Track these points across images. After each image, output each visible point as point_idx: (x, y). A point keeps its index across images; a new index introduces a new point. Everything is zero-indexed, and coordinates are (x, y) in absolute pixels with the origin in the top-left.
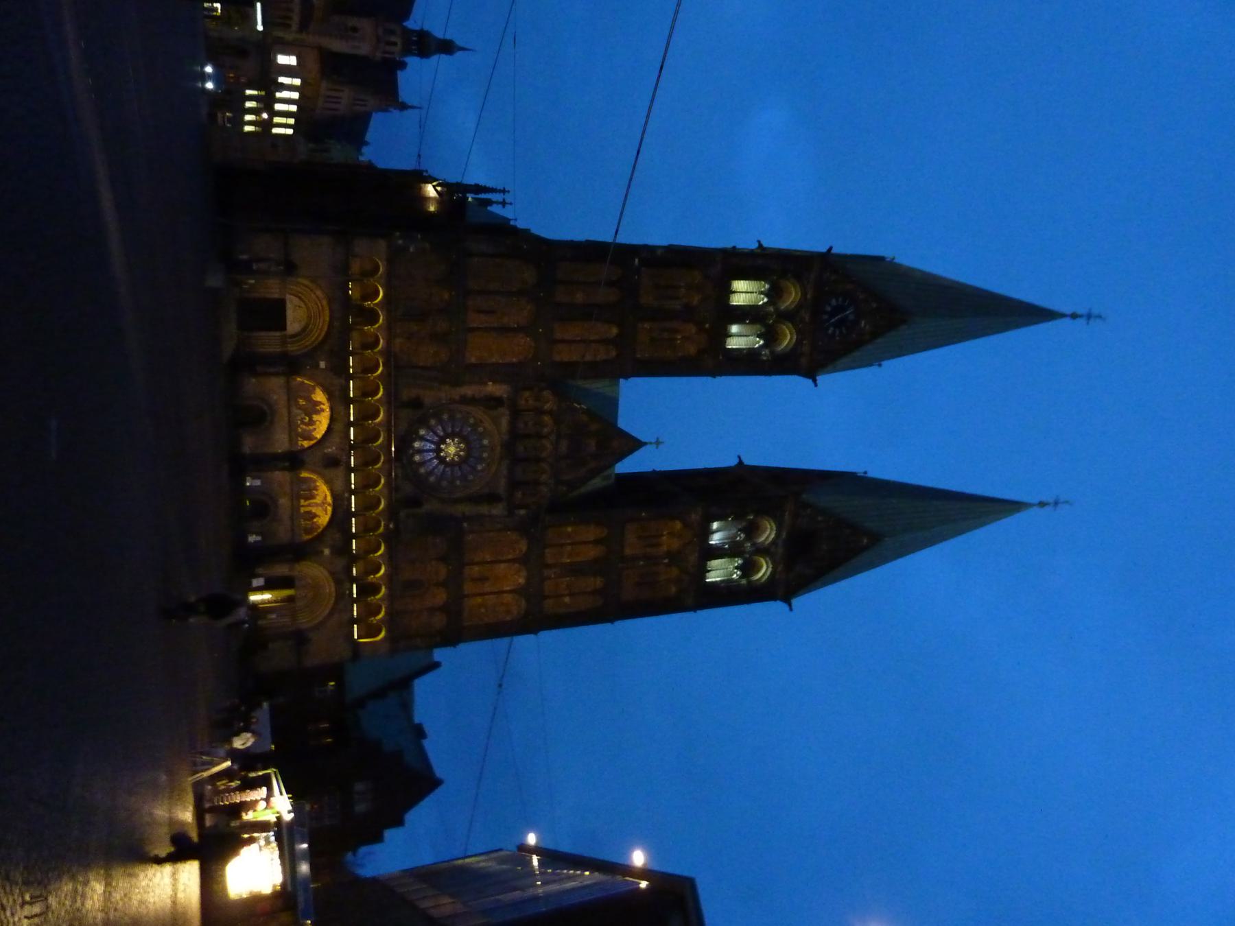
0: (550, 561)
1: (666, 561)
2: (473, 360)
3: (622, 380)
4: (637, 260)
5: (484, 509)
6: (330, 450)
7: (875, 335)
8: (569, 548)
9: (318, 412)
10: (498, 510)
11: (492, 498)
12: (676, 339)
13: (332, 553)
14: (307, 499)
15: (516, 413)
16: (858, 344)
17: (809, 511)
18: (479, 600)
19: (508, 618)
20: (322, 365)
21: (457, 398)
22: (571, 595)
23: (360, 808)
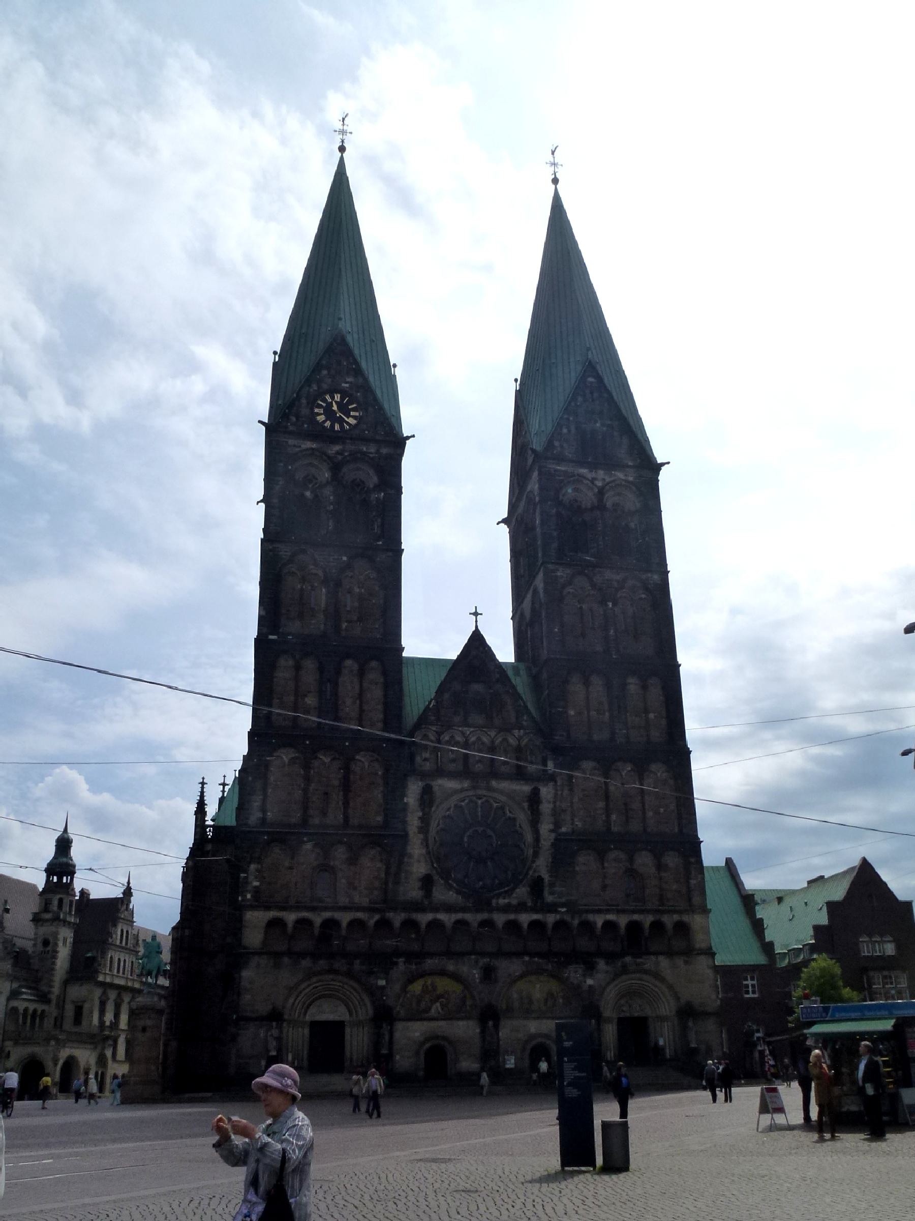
1: (610, 604)
2: (380, 819)
3: (404, 654)
4: (271, 637)
5: (546, 808)
6: (477, 976)
7: (358, 372)
8: (593, 713)
9: (434, 988)
10: (546, 792)
11: (534, 799)
13: (591, 976)
14: (531, 1002)
15: (440, 772)
17: (557, 444)
18: (650, 814)
19: (671, 782)
20: (382, 982)
21: (421, 836)
22: (646, 711)
23: (890, 949)
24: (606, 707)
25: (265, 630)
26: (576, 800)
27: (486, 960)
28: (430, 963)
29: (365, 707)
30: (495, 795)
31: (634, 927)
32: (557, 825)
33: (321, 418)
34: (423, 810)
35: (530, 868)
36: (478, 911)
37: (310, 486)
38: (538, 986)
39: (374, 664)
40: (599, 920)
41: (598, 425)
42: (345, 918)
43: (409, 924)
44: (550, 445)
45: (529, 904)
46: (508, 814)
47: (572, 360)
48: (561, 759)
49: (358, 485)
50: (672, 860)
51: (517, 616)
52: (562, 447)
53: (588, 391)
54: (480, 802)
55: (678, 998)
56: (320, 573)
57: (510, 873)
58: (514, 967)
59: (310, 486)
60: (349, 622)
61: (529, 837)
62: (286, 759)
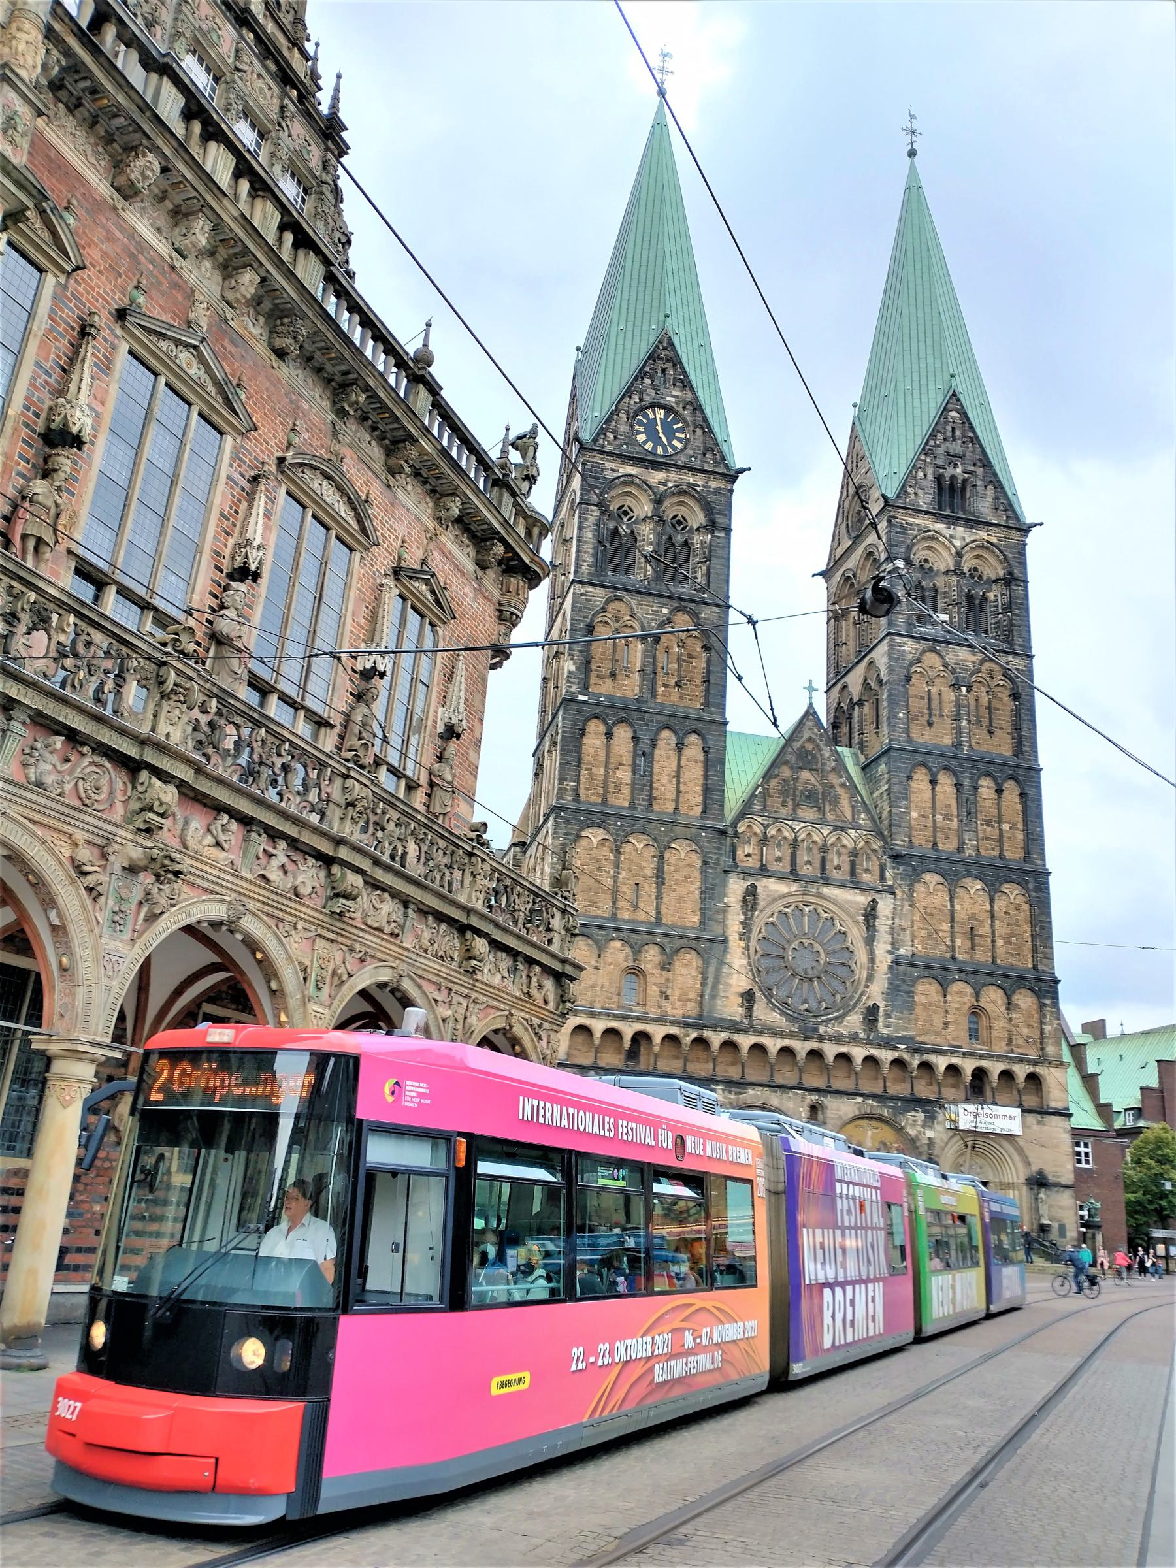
0: (952, 845)
1: (964, 689)
2: (696, 919)
3: (728, 728)
4: (581, 697)
5: (883, 924)
7: (685, 383)
8: (939, 818)
10: (885, 906)
11: (870, 914)
12: (680, 655)
13: (931, 1127)
15: (764, 871)
16: (697, 408)
17: (910, 490)
18: (1000, 942)
19: (1026, 907)
21: (742, 944)
22: (1000, 821)
24: (955, 812)
25: (574, 688)
26: (916, 918)
27: (815, 1097)
28: (752, 1094)
29: (682, 788)
30: (825, 904)
31: (980, 1074)
32: (895, 945)
33: (641, 438)
34: (745, 914)
35: (863, 994)
36: (807, 1038)
37: (625, 519)
38: (869, 1133)
39: (694, 738)
40: (941, 1063)
41: (959, 471)
42: (658, 1032)
43: (729, 1045)
44: (903, 492)
45: (861, 1036)
46: (839, 927)
47: (931, 386)
48: (901, 868)
49: (679, 523)
50: (1025, 1000)
51: (836, 691)
52: (916, 494)
53: (949, 428)
54: (807, 909)
55: (1028, 1163)
56: (636, 625)
57: (838, 997)
58: (846, 1108)
59: (625, 519)
60: (665, 686)
61: (862, 956)
62: (595, 841)
